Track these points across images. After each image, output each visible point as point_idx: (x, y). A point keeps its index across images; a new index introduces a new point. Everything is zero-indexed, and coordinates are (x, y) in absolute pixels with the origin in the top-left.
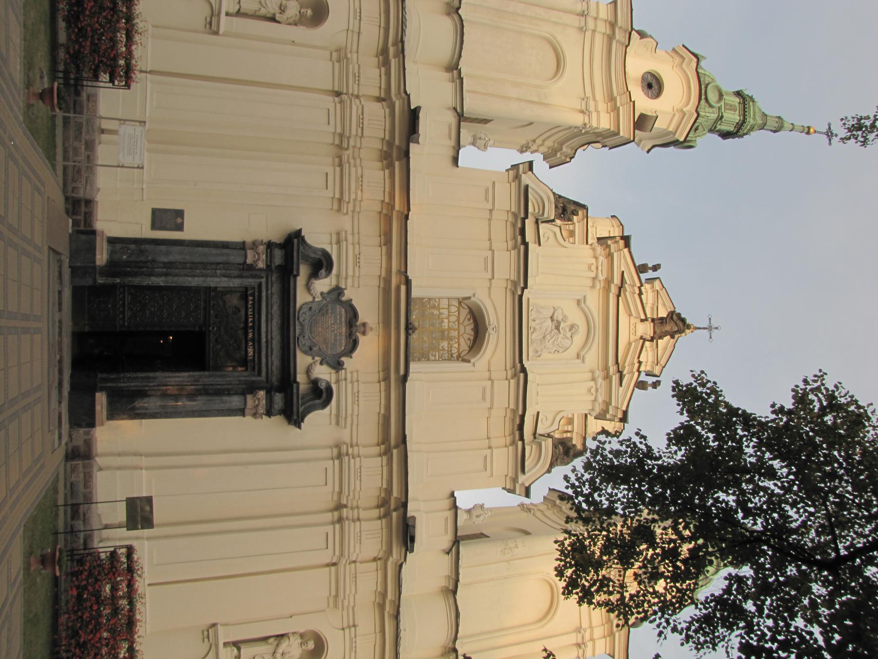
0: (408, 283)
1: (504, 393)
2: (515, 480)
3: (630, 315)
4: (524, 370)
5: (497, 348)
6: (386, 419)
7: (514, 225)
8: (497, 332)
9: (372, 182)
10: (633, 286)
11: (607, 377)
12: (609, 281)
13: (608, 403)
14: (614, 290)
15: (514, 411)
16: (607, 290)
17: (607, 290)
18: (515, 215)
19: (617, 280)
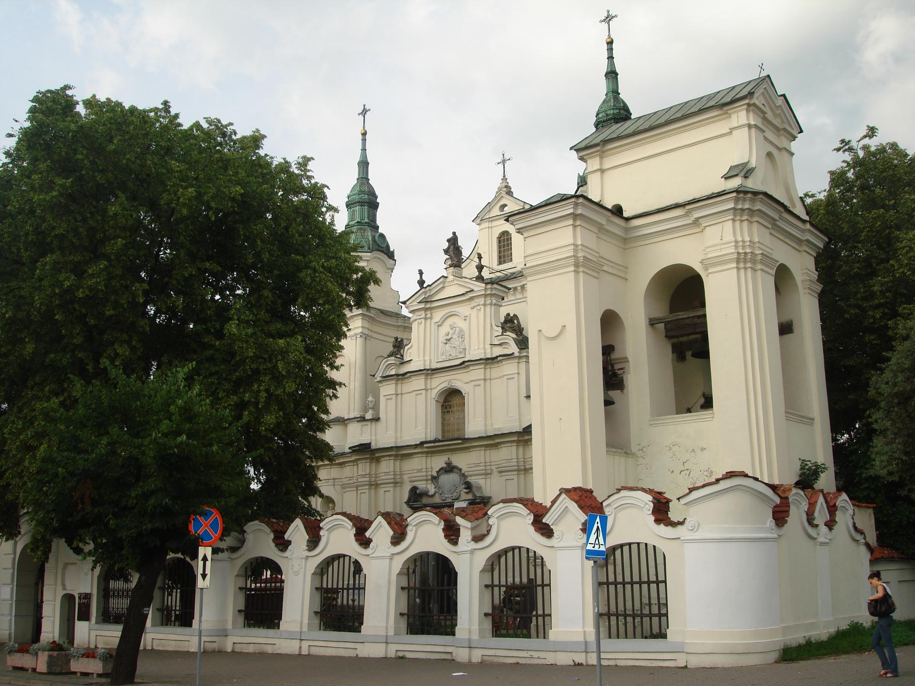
0: (422, 443)
1: (477, 373)
2: (520, 357)
3: (443, 287)
4: (463, 363)
5: (458, 380)
6: (486, 446)
7: (403, 379)
8: (450, 381)
9: (387, 466)
10: (425, 293)
11: (472, 299)
12: (426, 309)
13: (485, 296)
14: (428, 306)
15: (486, 364)
16: (431, 309)
17: (431, 309)
18: (398, 380)
19: (422, 306)
